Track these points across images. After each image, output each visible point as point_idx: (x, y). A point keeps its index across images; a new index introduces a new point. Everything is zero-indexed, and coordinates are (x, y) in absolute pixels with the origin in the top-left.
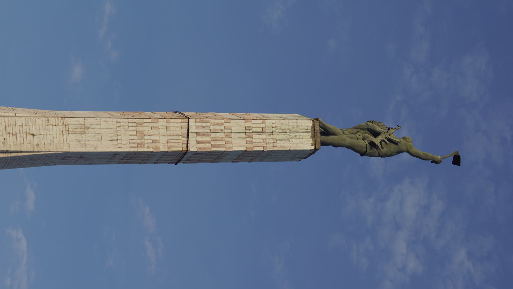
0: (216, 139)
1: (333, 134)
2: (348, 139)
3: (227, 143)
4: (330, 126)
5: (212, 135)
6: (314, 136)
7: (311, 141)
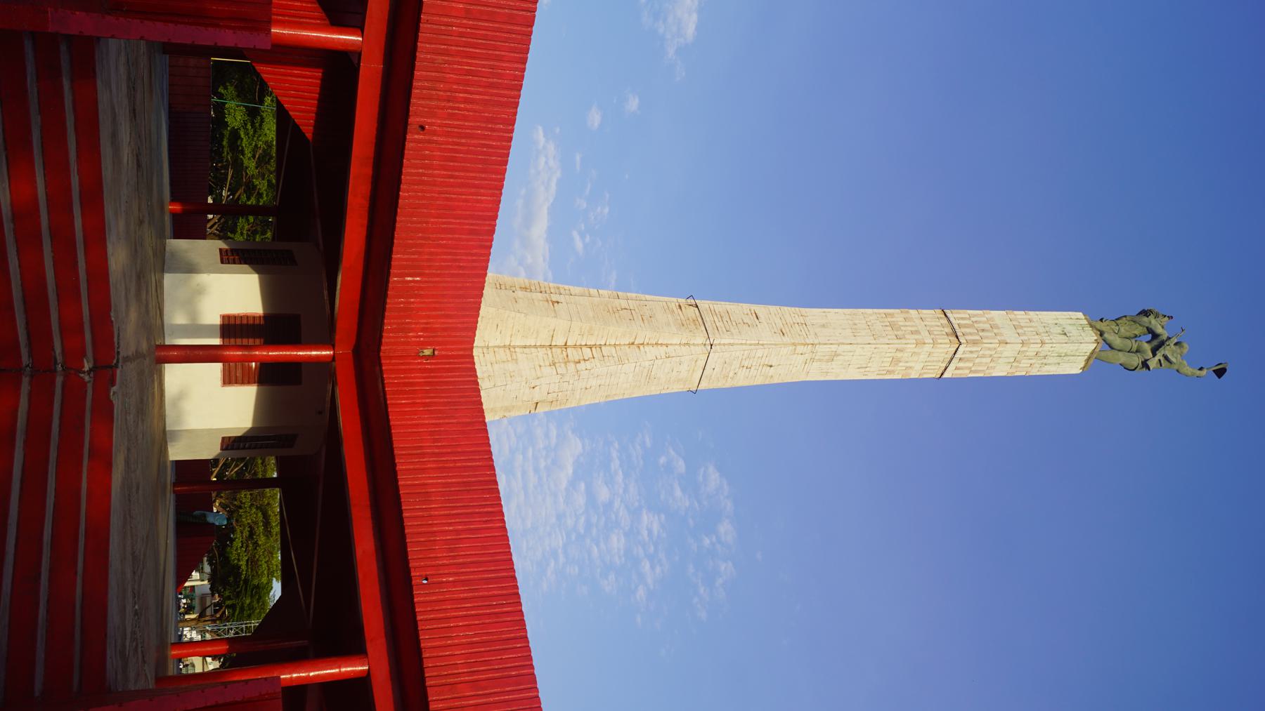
0: (980, 364)
5: (978, 360)
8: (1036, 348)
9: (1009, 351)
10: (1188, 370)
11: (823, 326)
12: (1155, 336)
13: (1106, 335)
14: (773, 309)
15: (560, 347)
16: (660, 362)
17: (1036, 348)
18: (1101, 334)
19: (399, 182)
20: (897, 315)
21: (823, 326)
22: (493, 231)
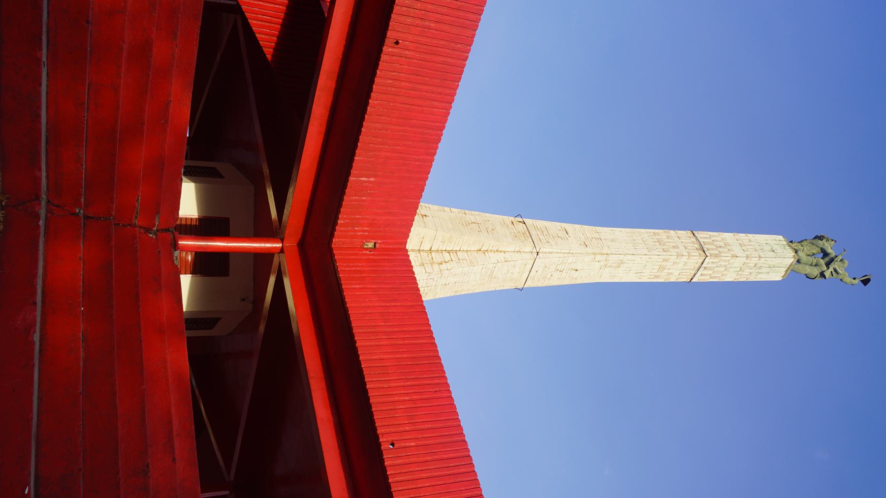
5: (716, 269)
8: (755, 260)
9: (737, 263)
10: (848, 280)
11: (613, 240)
12: (825, 254)
13: (799, 253)
14: (577, 226)
15: (426, 251)
16: (499, 265)
17: (755, 260)
18: (796, 252)
19: (370, 90)
20: (662, 233)
21: (613, 240)
22: (439, 140)
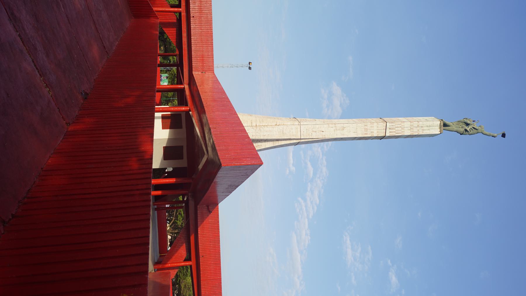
0: (398, 130)
1: (449, 126)
2: (454, 127)
3: (402, 132)
4: (448, 122)
5: (396, 129)
6: (440, 128)
7: (439, 130)
20: (364, 119)
